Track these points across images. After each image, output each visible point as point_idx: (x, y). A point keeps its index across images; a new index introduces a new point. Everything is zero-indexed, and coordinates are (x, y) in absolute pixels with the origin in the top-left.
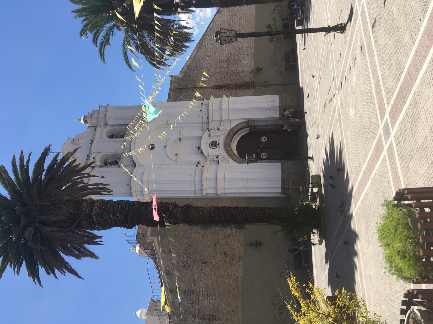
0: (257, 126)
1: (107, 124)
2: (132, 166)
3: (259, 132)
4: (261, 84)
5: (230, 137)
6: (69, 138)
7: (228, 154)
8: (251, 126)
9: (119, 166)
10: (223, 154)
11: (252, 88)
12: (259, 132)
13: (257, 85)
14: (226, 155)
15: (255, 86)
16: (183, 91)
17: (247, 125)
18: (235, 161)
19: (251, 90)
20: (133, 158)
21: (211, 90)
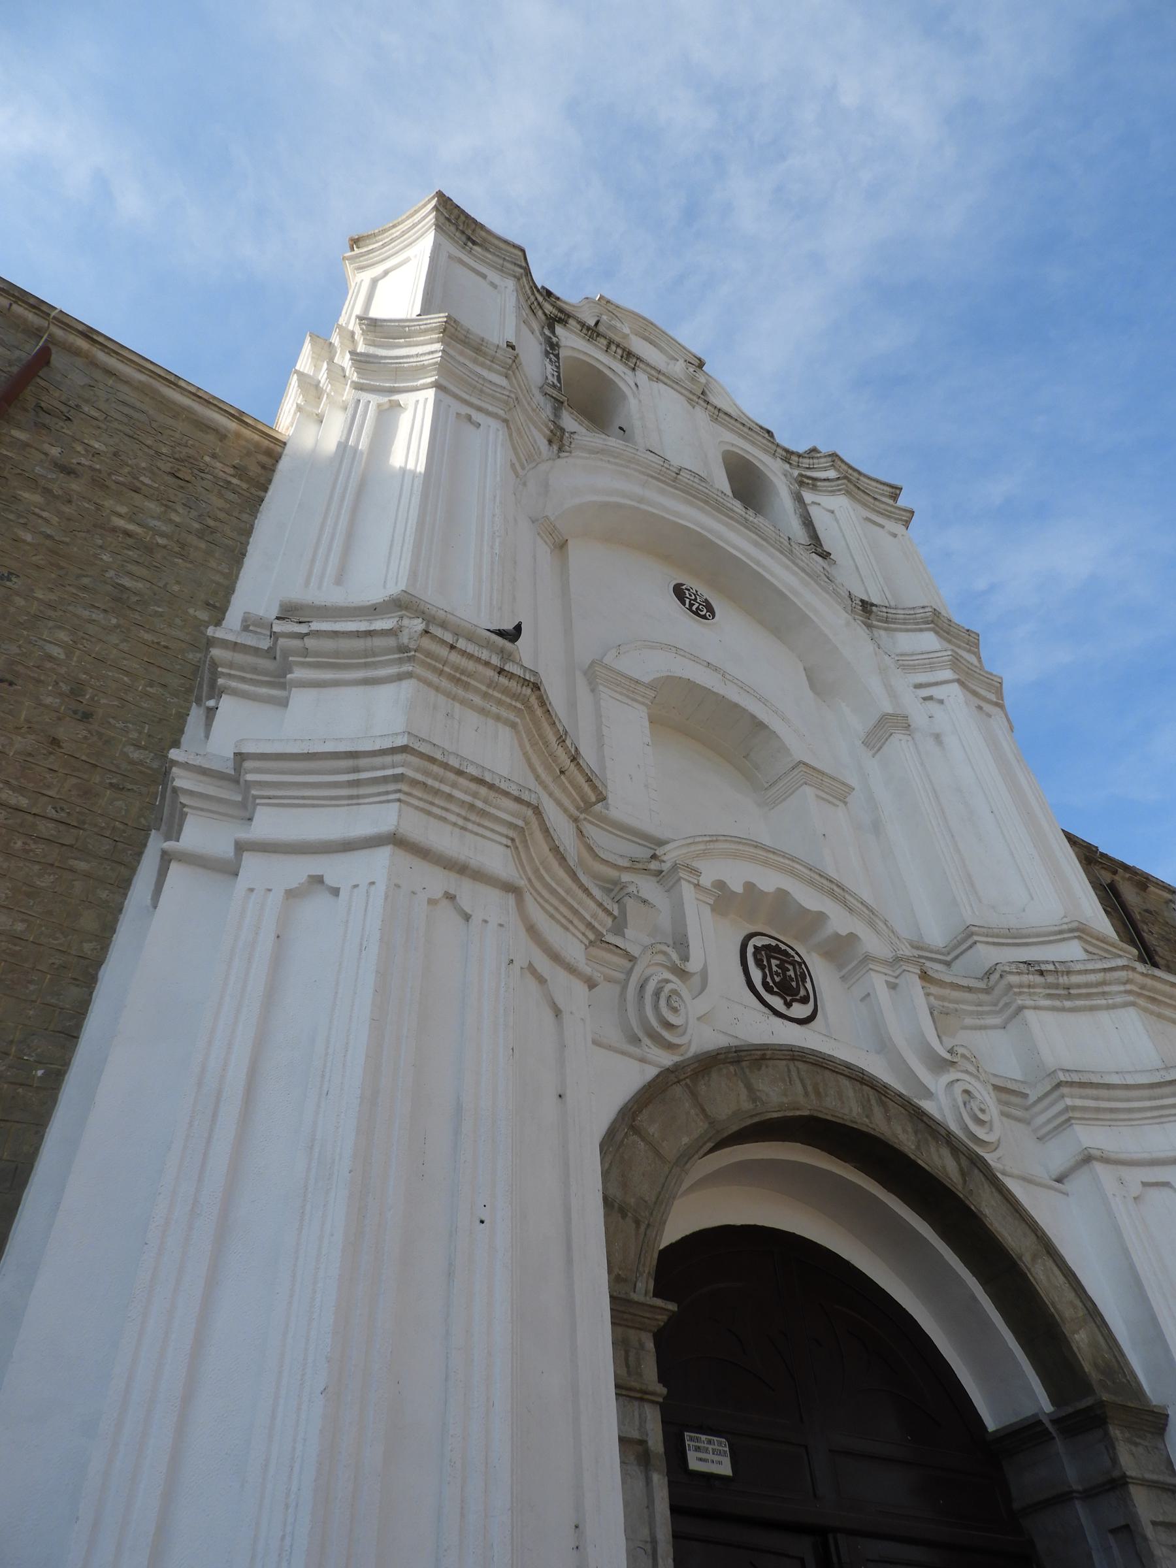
0: (1128, 1531)
1: (801, 484)
5: (904, 1138)
17: (1087, 1367)
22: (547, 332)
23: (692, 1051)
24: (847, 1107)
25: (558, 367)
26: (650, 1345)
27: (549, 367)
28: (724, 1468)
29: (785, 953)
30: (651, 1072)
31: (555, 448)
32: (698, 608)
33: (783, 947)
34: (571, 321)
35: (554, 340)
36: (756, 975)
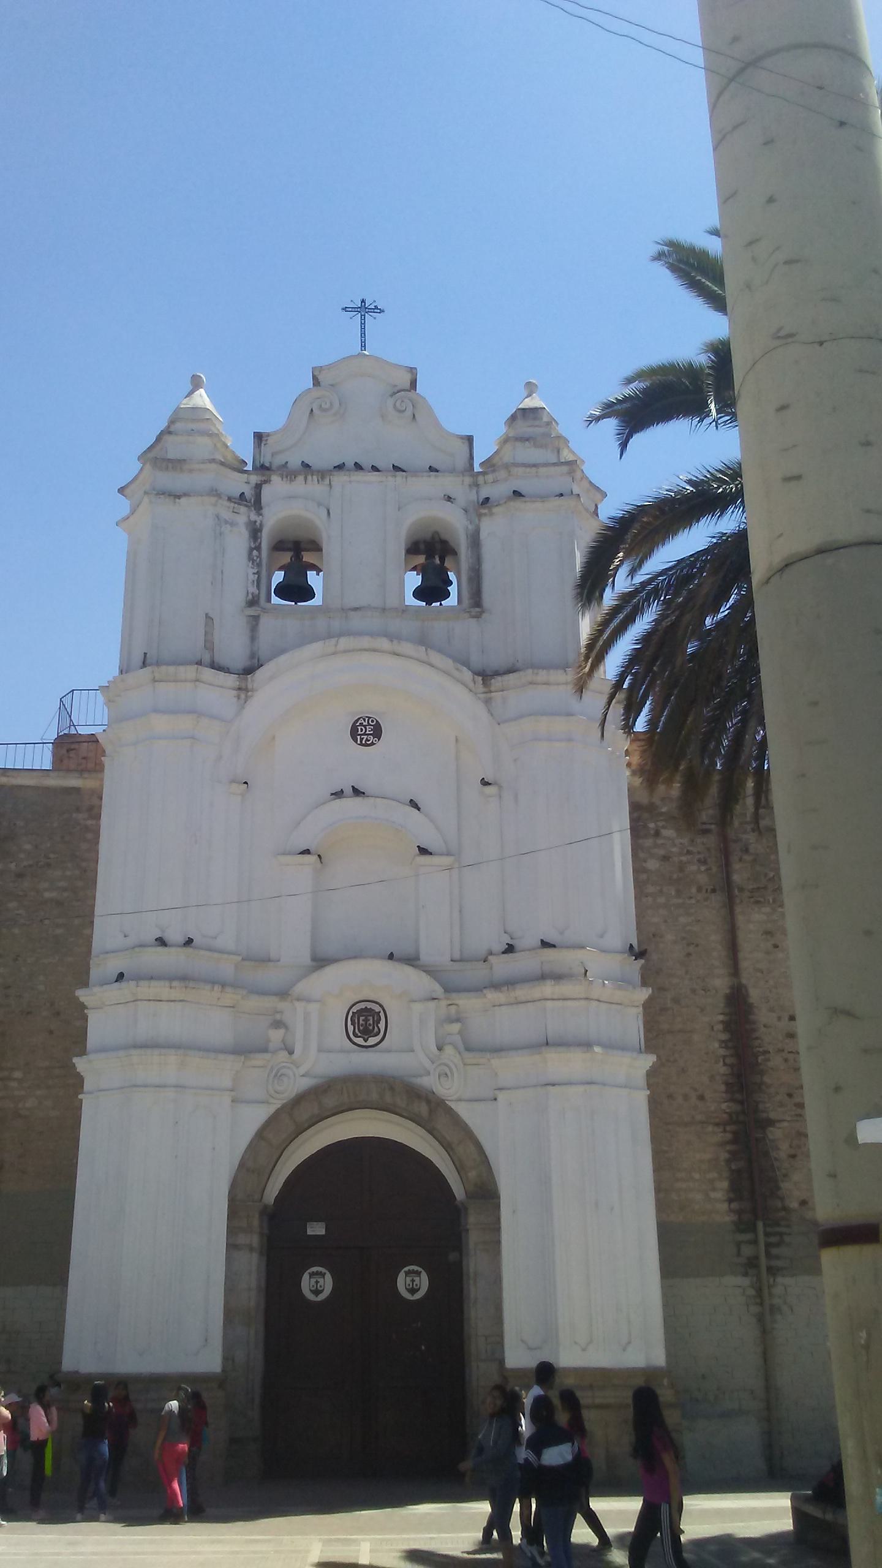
1: (480, 516)
2: (253, 655)
3: (453, 1257)
4: (763, 1262)
6: (413, 371)
7: (299, 1100)
8: (466, 1209)
9: (253, 602)
10: (302, 1070)
11: (740, 1212)
12: (453, 1257)
13: (755, 1242)
14: (296, 1083)
15: (753, 1229)
16: (712, 840)
18: (260, 1135)
19: (725, 1206)
20: (283, 658)
21: (721, 983)
22: (253, 517)
23: (293, 1095)
24: (375, 1096)
25: (259, 565)
26: (257, 1216)
27: (251, 571)
28: (322, 1232)
29: (371, 1010)
30: (272, 1109)
31: (243, 696)
32: (367, 740)
33: (369, 1005)
34: (275, 478)
35: (258, 519)
36: (351, 1028)
